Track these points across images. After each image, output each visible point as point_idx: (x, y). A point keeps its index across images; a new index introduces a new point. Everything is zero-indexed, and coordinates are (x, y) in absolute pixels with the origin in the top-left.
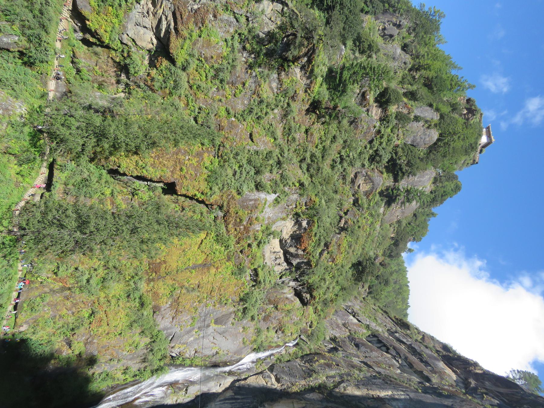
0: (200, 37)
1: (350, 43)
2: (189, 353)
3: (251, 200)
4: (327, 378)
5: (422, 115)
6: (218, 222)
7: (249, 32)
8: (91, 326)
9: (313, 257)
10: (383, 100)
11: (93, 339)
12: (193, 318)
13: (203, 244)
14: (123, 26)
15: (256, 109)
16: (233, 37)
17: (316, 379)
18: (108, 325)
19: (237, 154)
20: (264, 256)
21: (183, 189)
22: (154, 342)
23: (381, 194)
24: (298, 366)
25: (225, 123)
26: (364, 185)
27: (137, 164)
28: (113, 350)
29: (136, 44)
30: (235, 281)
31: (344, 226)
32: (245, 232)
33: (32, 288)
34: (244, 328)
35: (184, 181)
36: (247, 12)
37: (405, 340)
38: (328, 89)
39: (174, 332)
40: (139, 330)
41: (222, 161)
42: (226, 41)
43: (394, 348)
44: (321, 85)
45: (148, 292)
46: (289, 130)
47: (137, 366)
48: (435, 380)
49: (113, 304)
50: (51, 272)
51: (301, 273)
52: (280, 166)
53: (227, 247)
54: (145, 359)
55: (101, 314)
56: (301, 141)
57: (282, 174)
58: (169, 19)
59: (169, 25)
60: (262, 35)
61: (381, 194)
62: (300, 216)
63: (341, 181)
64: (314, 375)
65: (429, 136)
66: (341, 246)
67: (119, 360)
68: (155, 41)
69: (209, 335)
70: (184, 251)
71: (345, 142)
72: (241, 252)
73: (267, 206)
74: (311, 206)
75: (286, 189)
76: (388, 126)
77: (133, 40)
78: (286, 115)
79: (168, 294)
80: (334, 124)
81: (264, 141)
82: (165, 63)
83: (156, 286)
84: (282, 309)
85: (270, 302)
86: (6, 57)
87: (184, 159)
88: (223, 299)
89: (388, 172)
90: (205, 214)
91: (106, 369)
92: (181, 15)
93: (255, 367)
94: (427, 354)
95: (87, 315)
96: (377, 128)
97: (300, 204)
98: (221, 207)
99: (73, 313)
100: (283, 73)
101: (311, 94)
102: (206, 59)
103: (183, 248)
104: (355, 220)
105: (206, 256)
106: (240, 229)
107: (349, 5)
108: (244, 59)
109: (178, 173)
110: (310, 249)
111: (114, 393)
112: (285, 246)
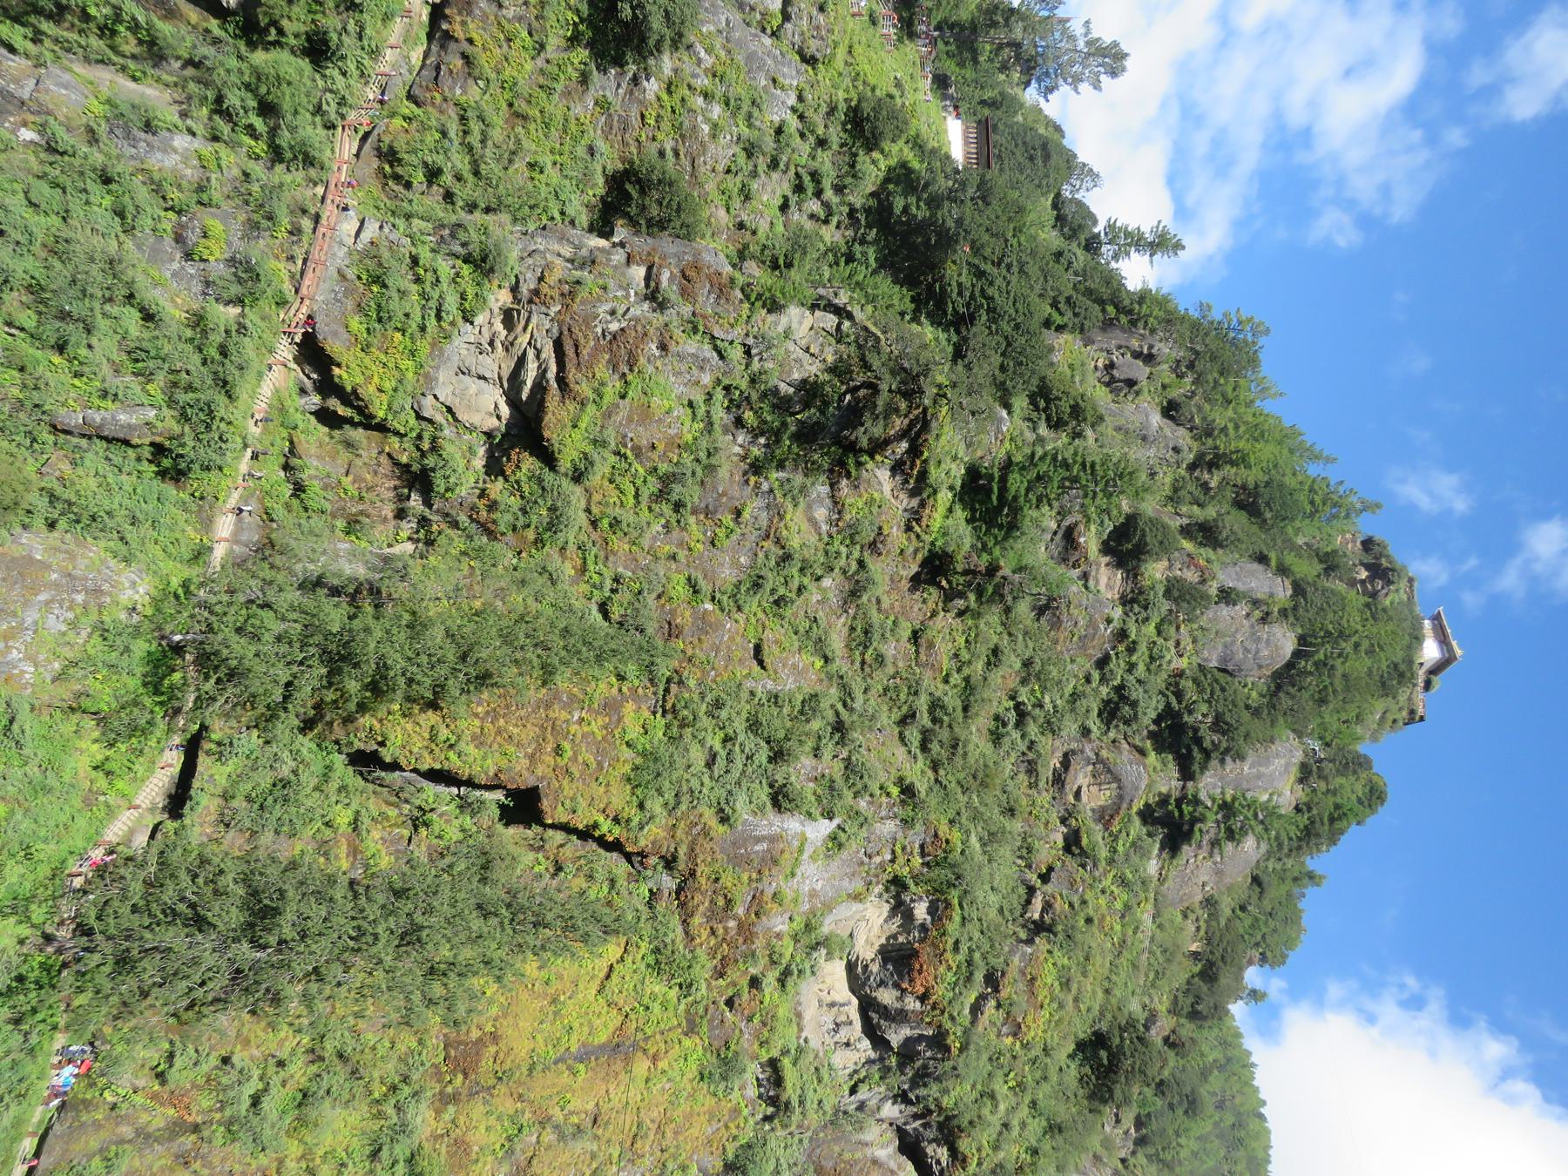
0: (623, 397)
1: (1020, 403)
3: (758, 840)
5: (1241, 587)
6: (661, 907)
7: (753, 381)
9: (952, 1018)
10: (1126, 546)
13: (614, 976)
14: (427, 376)
15: (772, 579)
16: (709, 396)
19: (718, 704)
20: (799, 1015)
21: (560, 808)
23: (1146, 815)
25: (685, 617)
26: (1094, 789)
27: (433, 738)
29: (456, 420)
30: (710, 1101)
31: (1042, 916)
32: (741, 940)
33: (83, 1125)
35: (565, 783)
36: (747, 335)
38: (968, 521)
41: (676, 723)
42: (691, 404)
44: (950, 510)
45: (436, 1138)
46: (866, 633)
50: (146, 1070)
51: (915, 1076)
52: (843, 738)
53: (686, 987)
56: (900, 664)
57: (848, 760)
58: (543, 356)
59: (545, 371)
60: (785, 389)
61: (1146, 815)
62: (905, 887)
63: (1022, 777)
65: (1268, 641)
68: (505, 411)
70: (554, 1001)
71: (1027, 664)
72: (730, 1003)
73: (806, 856)
74: (936, 855)
75: (862, 804)
76: (1147, 619)
77: (449, 410)
78: (854, 594)
79: (498, 1146)
80: (993, 616)
81: (795, 666)
82: (529, 463)
83: (462, 1119)
86: (117, 460)
87: (567, 721)
89: (1159, 749)
90: (622, 883)
92: (577, 347)
96: (1116, 624)
97: (904, 849)
98: (669, 863)
100: (844, 482)
101: (923, 536)
102: (638, 451)
103: (551, 991)
104: (1076, 900)
105: (620, 1018)
106: (726, 929)
107: (1012, 311)
108: (737, 449)
109: (550, 760)
110: (941, 992)
112: (864, 984)
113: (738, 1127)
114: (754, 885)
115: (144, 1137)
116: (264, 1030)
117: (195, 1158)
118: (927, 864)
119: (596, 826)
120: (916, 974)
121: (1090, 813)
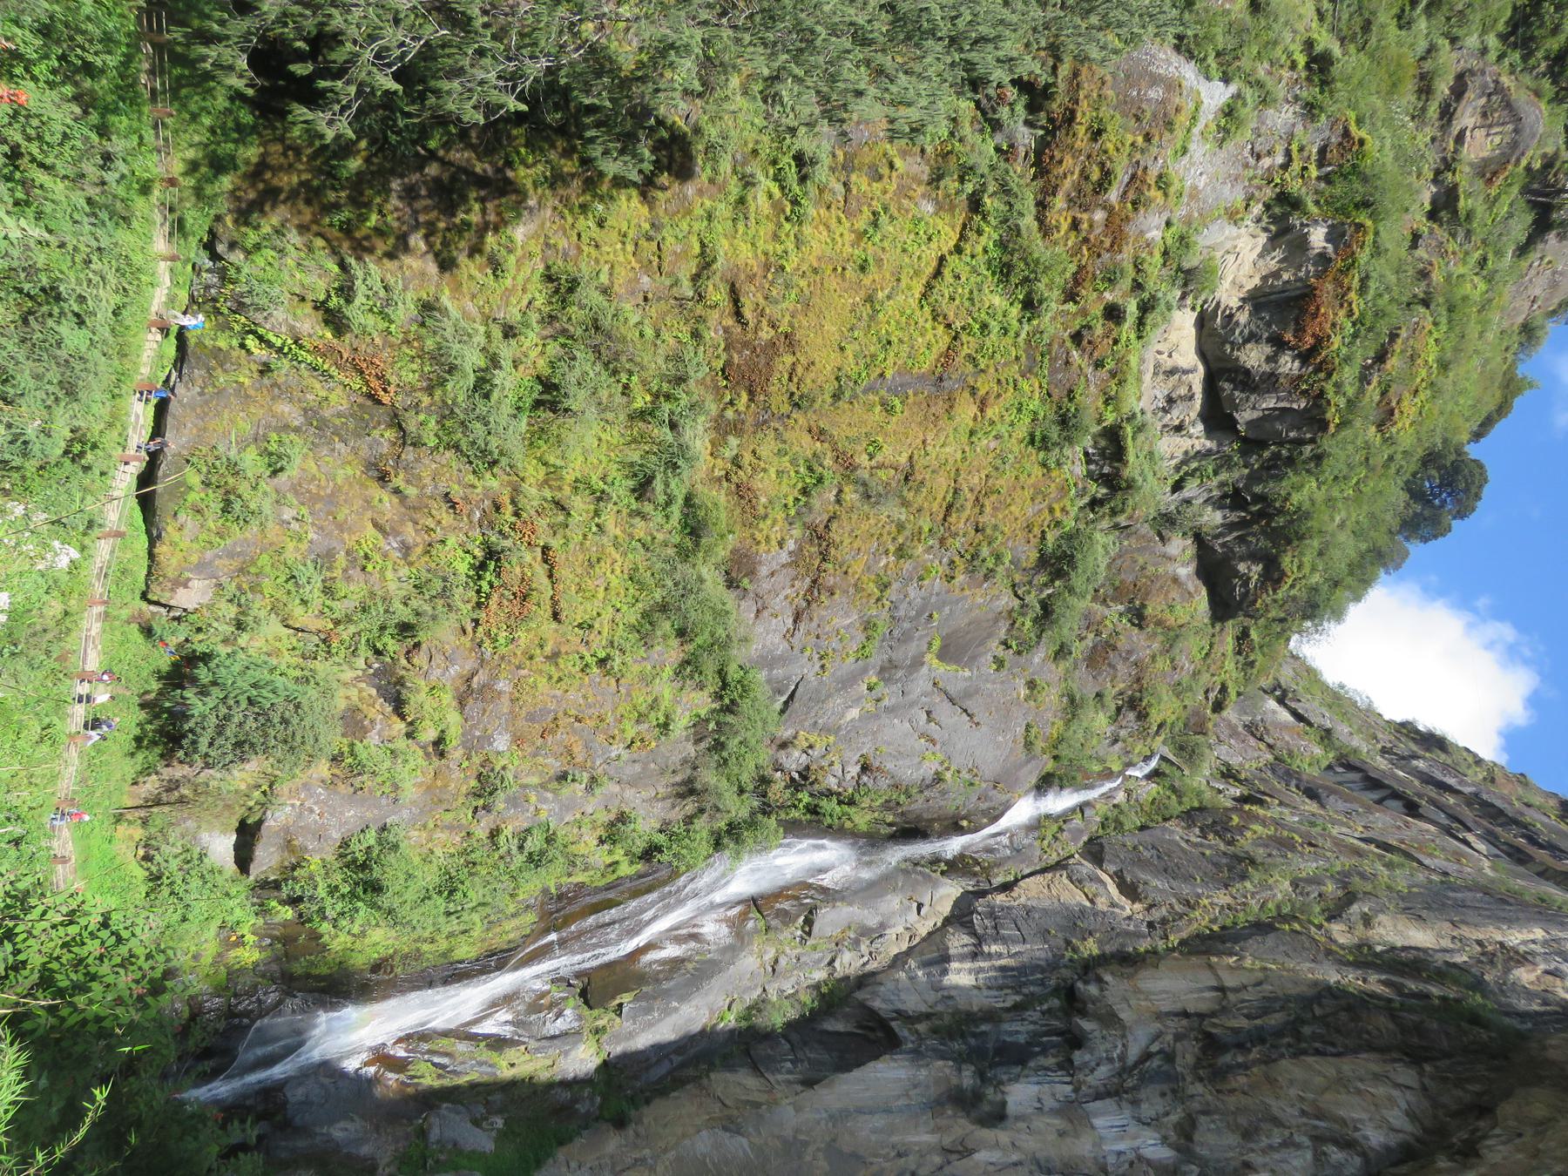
2: (839, 773)
4: (1295, 884)
8: (482, 615)
9: (1338, 385)
12: (868, 626)
13: (947, 272)
17: (1265, 886)
18: (556, 616)
22: (730, 709)
24: (1184, 845)
28: (575, 731)
30: (1038, 471)
32: (1107, 244)
33: (220, 392)
34: (1031, 685)
37: (1452, 781)
39: (796, 679)
40: (671, 652)
43: (1432, 802)
47: (660, 811)
49: (576, 517)
50: (308, 308)
51: (1262, 467)
54: (690, 781)
55: (523, 562)
64: (1256, 875)
66: (1419, 361)
67: (593, 779)
69: (912, 704)
70: (870, 299)
73: (1196, 130)
74: (1342, 160)
75: (1261, 71)
79: (791, 500)
83: (747, 458)
84: (1159, 623)
85: (1119, 593)
88: (985, 551)
91: (543, 816)
93: (1037, 843)
94: (1543, 824)
95: (463, 567)
97: (1301, 149)
99: (406, 549)
105: (947, 339)
111: (567, 921)
114: (1138, 156)
115: (317, 424)
116: (480, 269)
118: (1327, 179)
119: (813, 162)
120: (1307, 318)
121: (1467, 169)
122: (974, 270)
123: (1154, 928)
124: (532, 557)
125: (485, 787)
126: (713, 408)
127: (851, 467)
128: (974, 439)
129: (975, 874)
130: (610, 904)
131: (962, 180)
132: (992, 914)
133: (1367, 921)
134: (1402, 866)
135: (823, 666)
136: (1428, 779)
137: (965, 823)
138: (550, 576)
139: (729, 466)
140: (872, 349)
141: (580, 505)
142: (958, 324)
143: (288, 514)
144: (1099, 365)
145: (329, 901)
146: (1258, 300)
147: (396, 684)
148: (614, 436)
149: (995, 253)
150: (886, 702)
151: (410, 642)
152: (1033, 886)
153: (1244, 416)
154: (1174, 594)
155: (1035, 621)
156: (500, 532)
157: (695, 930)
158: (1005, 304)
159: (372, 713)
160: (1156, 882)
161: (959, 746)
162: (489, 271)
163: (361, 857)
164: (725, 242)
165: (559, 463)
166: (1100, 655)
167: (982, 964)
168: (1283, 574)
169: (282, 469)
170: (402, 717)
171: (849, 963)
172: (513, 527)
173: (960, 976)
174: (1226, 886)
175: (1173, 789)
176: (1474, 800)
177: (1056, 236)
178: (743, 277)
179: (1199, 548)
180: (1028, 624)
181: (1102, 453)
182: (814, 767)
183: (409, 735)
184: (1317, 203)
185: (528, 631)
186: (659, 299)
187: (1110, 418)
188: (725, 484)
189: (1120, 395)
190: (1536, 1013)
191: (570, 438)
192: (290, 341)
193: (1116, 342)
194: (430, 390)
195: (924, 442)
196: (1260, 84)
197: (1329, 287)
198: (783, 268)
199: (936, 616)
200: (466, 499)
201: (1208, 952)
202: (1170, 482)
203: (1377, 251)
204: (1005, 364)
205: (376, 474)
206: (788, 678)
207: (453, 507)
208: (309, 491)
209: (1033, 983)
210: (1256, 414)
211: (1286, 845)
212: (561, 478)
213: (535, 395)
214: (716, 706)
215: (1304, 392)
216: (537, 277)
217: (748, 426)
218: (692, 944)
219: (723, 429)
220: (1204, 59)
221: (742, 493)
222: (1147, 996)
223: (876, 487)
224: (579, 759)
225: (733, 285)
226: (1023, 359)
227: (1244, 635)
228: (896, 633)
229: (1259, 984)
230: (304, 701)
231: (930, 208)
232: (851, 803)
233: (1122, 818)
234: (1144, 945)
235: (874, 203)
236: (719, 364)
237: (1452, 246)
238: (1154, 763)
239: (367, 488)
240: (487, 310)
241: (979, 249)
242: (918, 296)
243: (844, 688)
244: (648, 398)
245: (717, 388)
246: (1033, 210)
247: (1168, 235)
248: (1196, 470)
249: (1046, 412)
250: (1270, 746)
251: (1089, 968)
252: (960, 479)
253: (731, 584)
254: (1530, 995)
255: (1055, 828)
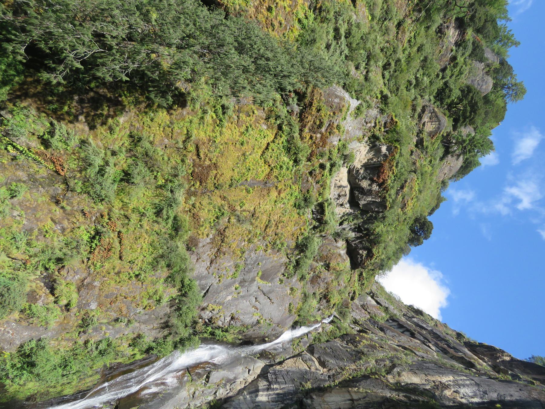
2: (222, 320)
4: (376, 361)
11: (94, 281)
12: (237, 266)
13: (270, 148)
17: (367, 362)
18: (120, 258)
22: (184, 295)
24: (341, 347)
28: (123, 302)
30: (297, 216)
32: (321, 145)
34: (292, 289)
35: (270, 30)
37: (425, 326)
39: (209, 285)
40: (164, 273)
43: (419, 333)
47: (154, 333)
48: (479, 367)
50: (35, 138)
51: (367, 219)
53: (296, 161)
54: (167, 322)
55: (110, 237)
65: (486, 82)
67: (129, 321)
69: (250, 295)
70: (244, 155)
73: (348, 113)
74: (391, 127)
75: (368, 98)
83: (198, 205)
84: (334, 269)
85: (322, 258)
88: (278, 242)
91: (107, 335)
93: (291, 347)
95: (86, 238)
97: (379, 122)
99: (63, 230)
109: (265, 13)
111: (113, 378)
112: (356, 178)
113: (304, 229)
114: (331, 119)
115: (33, 180)
116: (105, 131)
117: (63, 199)
118: (386, 132)
119: (228, 108)
121: (426, 134)
122: (278, 148)
123: (330, 378)
124: (113, 235)
125: (85, 323)
126: (187, 186)
127: (234, 210)
128: (276, 204)
129: (270, 358)
130: (131, 371)
131: (276, 119)
132: (275, 374)
133: (399, 374)
134: (410, 355)
135: (219, 280)
136: (417, 325)
137: (267, 339)
138: (120, 243)
139: (191, 207)
140: (244, 171)
141: (134, 217)
142: (273, 165)
143: (15, 213)
144: (317, 182)
145: (11, 370)
146: (366, 166)
147: (52, 282)
148: (149, 193)
149: (285, 144)
150: (241, 294)
151: (60, 265)
152: (289, 363)
153: (362, 203)
154: (339, 260)
155: (294, 267)
156: (102, 225)
157: (164, 381)
158: (288, 160)
159: (41, 293)
160: (332, 361)
161: (266, 311)
162: (108, 132)
163: (28, 352)
164: (195, 131)
165: (128, 201)
166: (315, 280)
167: (271, 393)
168: (373, 255)
169: (16, 196)
170: (53, 295)
171: (222, 393)
172: (107, 223)
173: (262, 397)
174: (354, 362)
175: (338, 327)
176: (431, 332)
177: (305, 140)
178: (201, 143)
179: (347, 245)
180: (292, 268)
181: (317, 211)
182: (214, 317)
183: (55, 302)
184: (384, 139)
185: (109, 263)
186: (171, 147)
187: (320, 200)
188: (189, 213)
189: (324, 193)
190: (451, 406)
191: (133, 193)
192: (26, 149)
193: (323, 176)
194: (80, 172)
195: (259, 203)
196: (367, 102)
197: (387, 164)
198: (215, 142)
199: (260, 264)
200: (90, 212)
201: (348, 386)
202: (339, 222)
203: (401, 155)
204: (287, 180)
205: (55, 201)
206: (207, 284)
207: (85, 215)
208: (26, 205)
209: (288, 399)
210: (365, 202)
211: (373, 347)
212: (128, 207)
213: (121, 177)
214: (179, 294)
215: (380, 197)
216: (126, 135)
217: (199, 194)
218: (162, 387)
219: (190, 194)
220: (351, 92)
221: (195, 217)
222: (328, 403)
223: (242, 218)
224: (124, 313)
225: (197, 145)
226: (293, 178)
227: (361, 275)
228: (246, 269)
229: (364, 398)
230: (12, 288)
231: (265, 127)
232: (227, 331)
233: (320, 337)
234: (327, 384)
235: (247, 124)
236: (191, 171)
237: (422, 156)
238: (331, 318)
239: (50, 205)
240: (106, 145)
241: (281, 142)
242: (260, 155)
243: (227, 288)
244: (164, 181)
245: (189, 180)
246: (298, 131)
247: (340, 143)
248: (347, 219)
249: (300, 196)
250: (369, 313)
251: (308, 393)
252: (271, 217)
253: (188, 249)
254: (449, 400)
255: (298, 341)
